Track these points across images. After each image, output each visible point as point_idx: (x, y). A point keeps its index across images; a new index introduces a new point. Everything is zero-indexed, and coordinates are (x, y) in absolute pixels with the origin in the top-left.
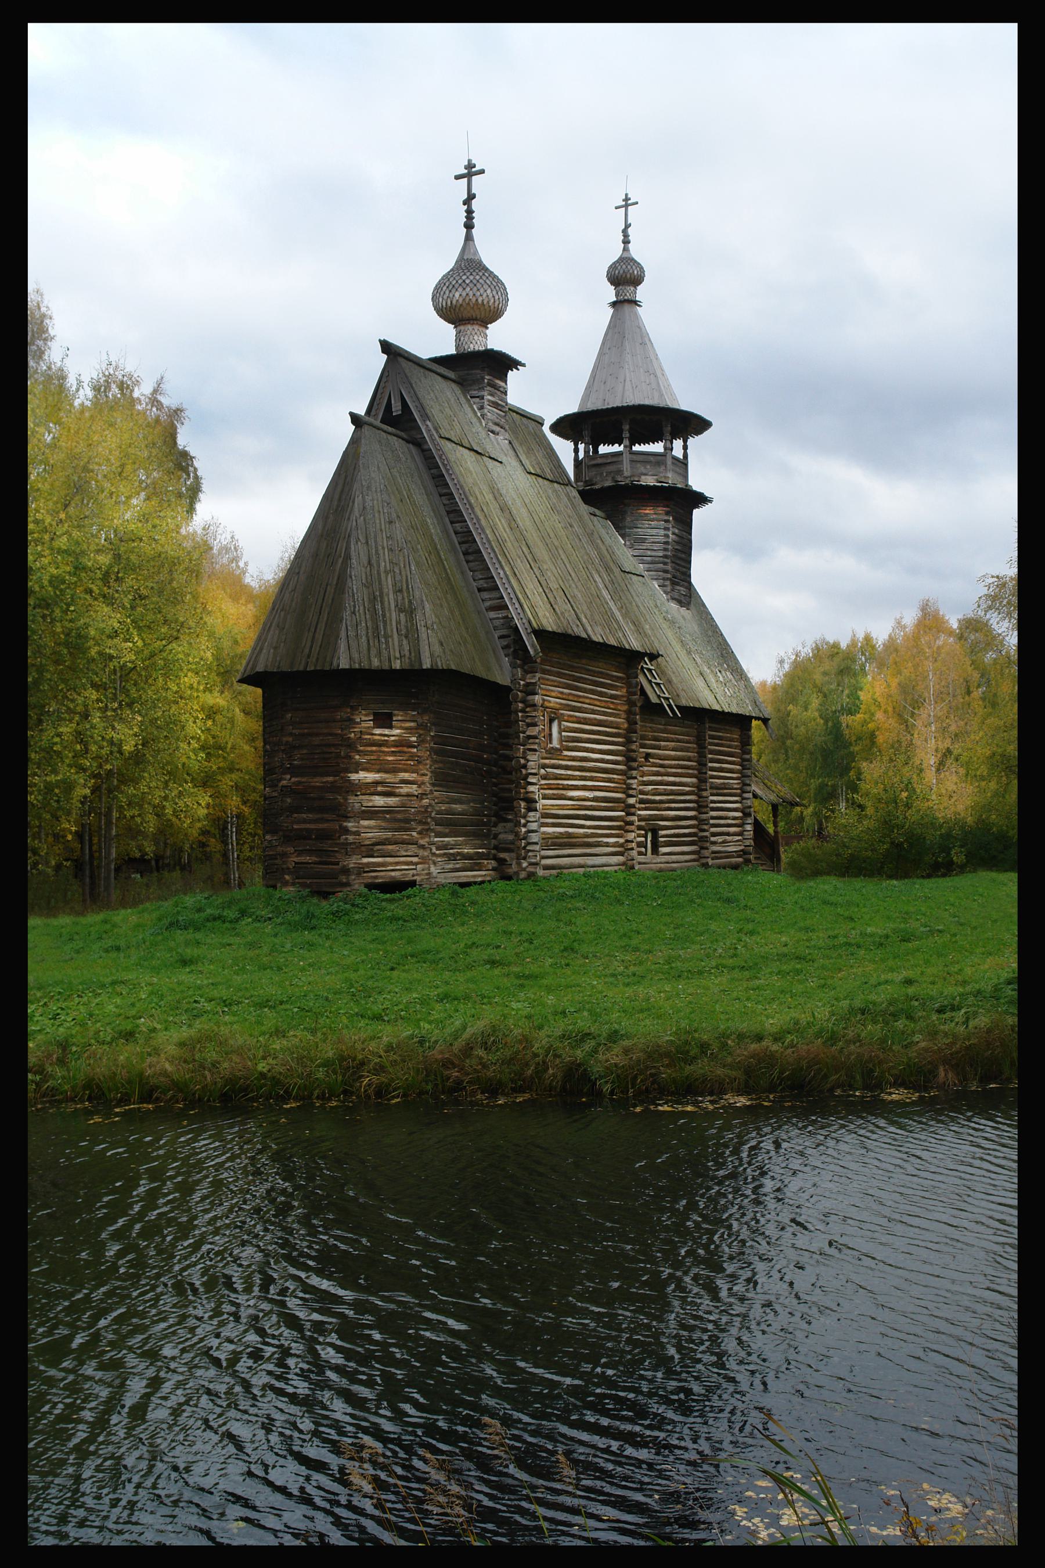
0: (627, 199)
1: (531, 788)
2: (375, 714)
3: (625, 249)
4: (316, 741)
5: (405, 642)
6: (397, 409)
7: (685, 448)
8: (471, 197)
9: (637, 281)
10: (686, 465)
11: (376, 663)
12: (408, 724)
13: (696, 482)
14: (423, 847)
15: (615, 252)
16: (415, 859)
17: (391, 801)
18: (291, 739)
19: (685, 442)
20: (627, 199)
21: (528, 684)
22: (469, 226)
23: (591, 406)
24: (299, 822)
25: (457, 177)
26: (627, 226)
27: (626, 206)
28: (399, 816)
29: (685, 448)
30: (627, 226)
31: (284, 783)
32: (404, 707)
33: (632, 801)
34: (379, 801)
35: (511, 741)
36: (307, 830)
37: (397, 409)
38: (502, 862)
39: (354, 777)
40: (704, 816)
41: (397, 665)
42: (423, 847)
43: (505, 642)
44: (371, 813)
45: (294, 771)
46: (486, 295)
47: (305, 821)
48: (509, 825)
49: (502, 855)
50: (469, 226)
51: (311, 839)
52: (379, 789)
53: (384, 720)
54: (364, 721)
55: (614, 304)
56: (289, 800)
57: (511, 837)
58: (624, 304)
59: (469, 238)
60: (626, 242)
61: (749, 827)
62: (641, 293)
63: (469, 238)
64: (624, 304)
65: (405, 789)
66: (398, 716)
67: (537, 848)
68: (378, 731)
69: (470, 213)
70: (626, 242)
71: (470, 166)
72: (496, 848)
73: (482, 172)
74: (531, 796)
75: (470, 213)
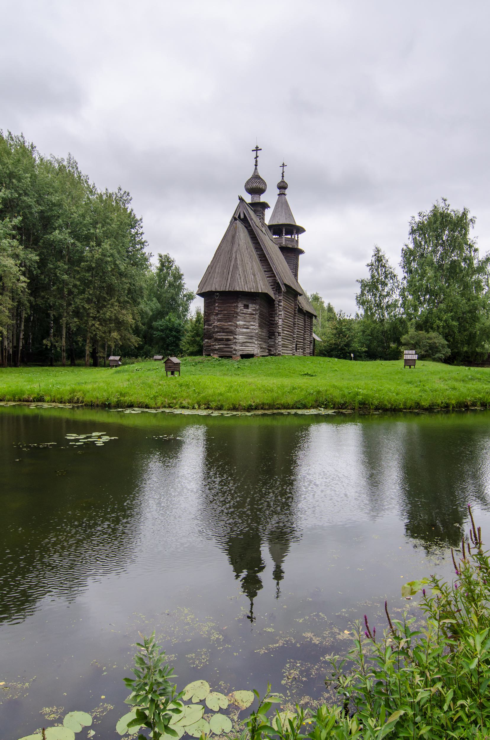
0: (283, 164)
1: (279, 329)
2: (244, 305)
3: (283, 179)
4: (226, 312)
5: (254, 284)
6: (242, 216)
7: (298, 237)
8: (257, 157)
9: (285, 188)
10: (298, 242)
11: (247, 290)
12: (253, 308)
13: (300, 247)
14: (256, 344)
15: (280, 180)
16: (254, 348)
17: (248, 330)
18: (217, 311)
19: (298, 236)
20: (283, 164)
21: (280, 299)
22: (256, 165)
23: (271, 224)
24: (219, 336)
25: (253, 151)
26: (283, 172)
27: (283, 166)
28: (250, 335)
29: (298, 237)
30: (283, 172)
31: (215, 324)
32: (252, 303)
33: (295, 336)
34: (245, 330)
35: (274, 316)
37: (242, 216)
38: (270, 350)
39: (238, 323)
40: (305, 342)
41: (252, 291)
42: (256, 344)
43: (273, 287)
44: (243, 334)
45: (219, 320)
46: (262, 186)
47: (221, 336)
48: (273, 340)
49: (271, 348)
50: (256, 165)
51: (223, 340)
52: (245, 327)
53: (246, 307)
54: (241, 306)
55: (279, 195)
56: (216, 329)
57: (273, 343)
59: (256, 169)
60: (283, 177)
61: (312, 346)
62: (287, 192)
63: (256, 169)
65: (252, 327)
66: (250, 305)
67: (281, 346)
68: (245, 310)
69: (256, 161)
70: (283, 177)
71: (257, 147)
72: (268, 346)
73: (261, 150)
74: (279, 332)
75: (256, 161)
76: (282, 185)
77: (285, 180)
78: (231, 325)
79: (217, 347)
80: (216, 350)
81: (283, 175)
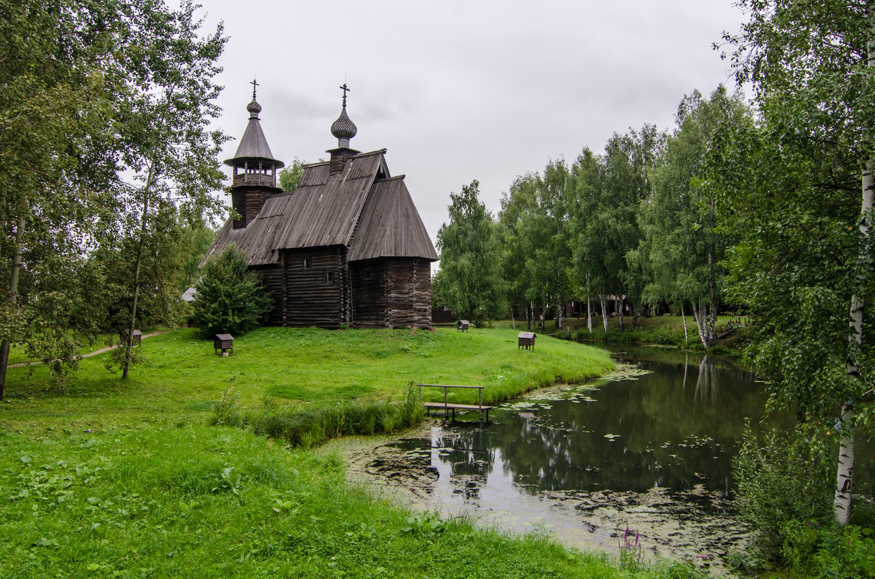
0: (255, 82)
3: (254, 99)
8: (345, 97)
15: (251, 100)
20: (255, 82)
22: (344, 106)
23: (241, 156)
26: (255, 92)
27: (255, 84)
30: (255, 92)
37: (382, 171)
45: (417, 289)
50: (344, 106)
55: (250, 119)
58: (254, 119)
59: (344, 110)
60: (254, 97)
62: (260, 115)
63: (344, 110)
64: (254, 119)
69: (344, 101)
70: (254, 97)
71: (345, 86)
75: (344, 101)
76: (253, 107)
77: (258, 100)
78: (427, 295)
79: (416, 318)
81: (254, 94)
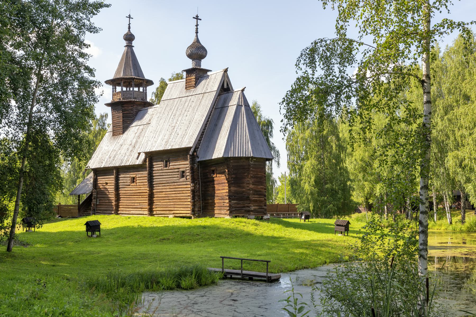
0: (130, 16)
3: (129, 30)
8: (197, 25)
15: (126, 31)
23: (118, 77)
24: (254, 197)
26: (129, 24)
27: (130, 18)
30: (129, 24)
36: (257, 200)
37: (225, 86)
55: (126, 46)
58: (130, 46)
59: (197, 36)
60: (129, 28)
62: (134, 43)
63: (197, 36)
64: (130, 46)
69: (197, 29)
70: (129, 28)
75: (197, 29)
77: (132, 31)
79: (252, 208)
80: (252, 211)
81: (129, 26)
